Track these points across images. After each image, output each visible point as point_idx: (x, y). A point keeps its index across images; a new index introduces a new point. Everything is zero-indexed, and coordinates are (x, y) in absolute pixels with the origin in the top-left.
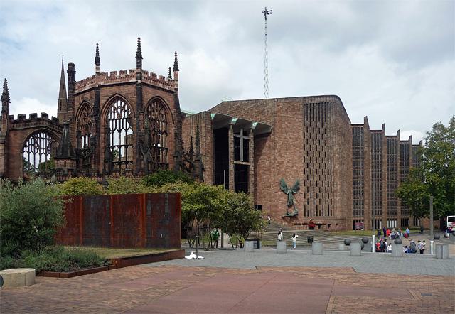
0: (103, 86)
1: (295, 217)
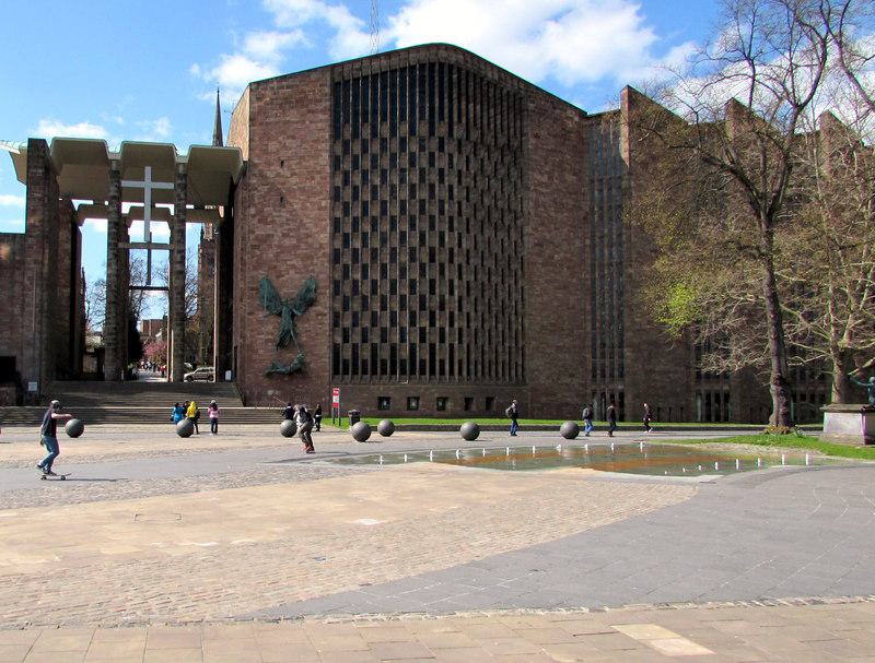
1: (299, 372)
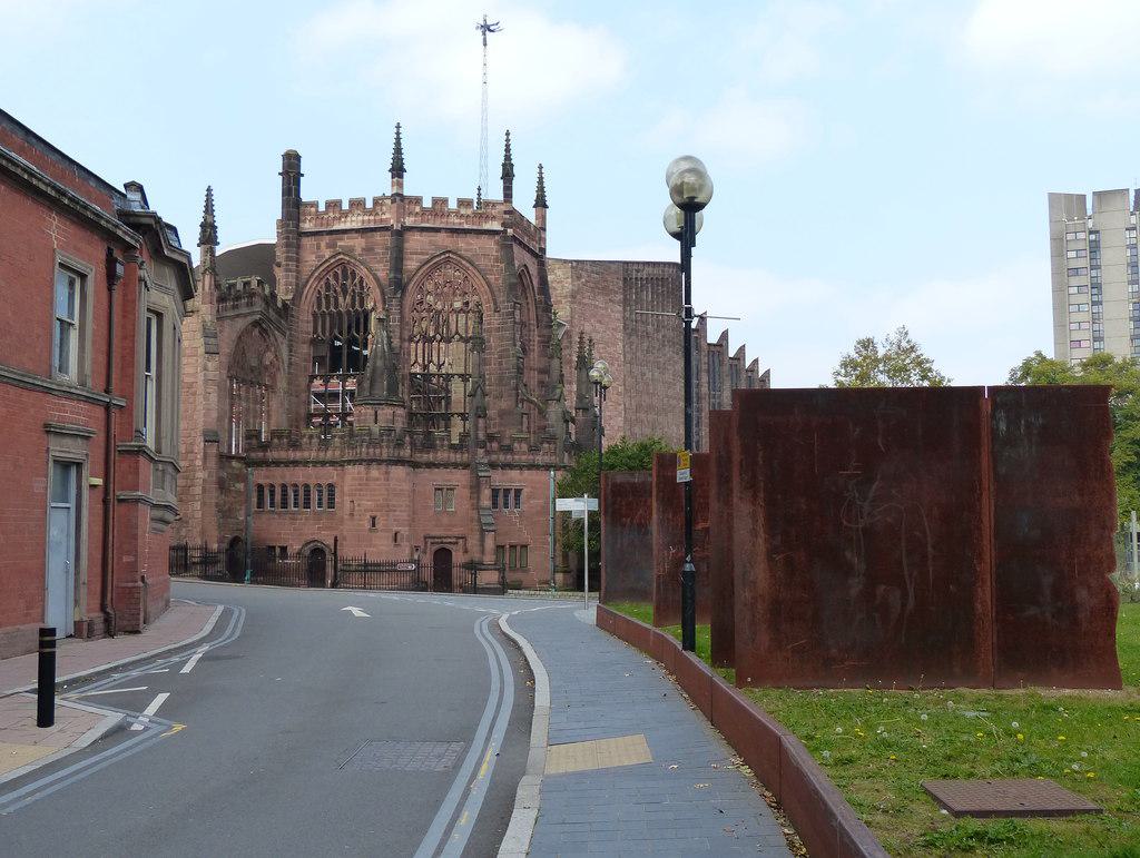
0: (411, 229)
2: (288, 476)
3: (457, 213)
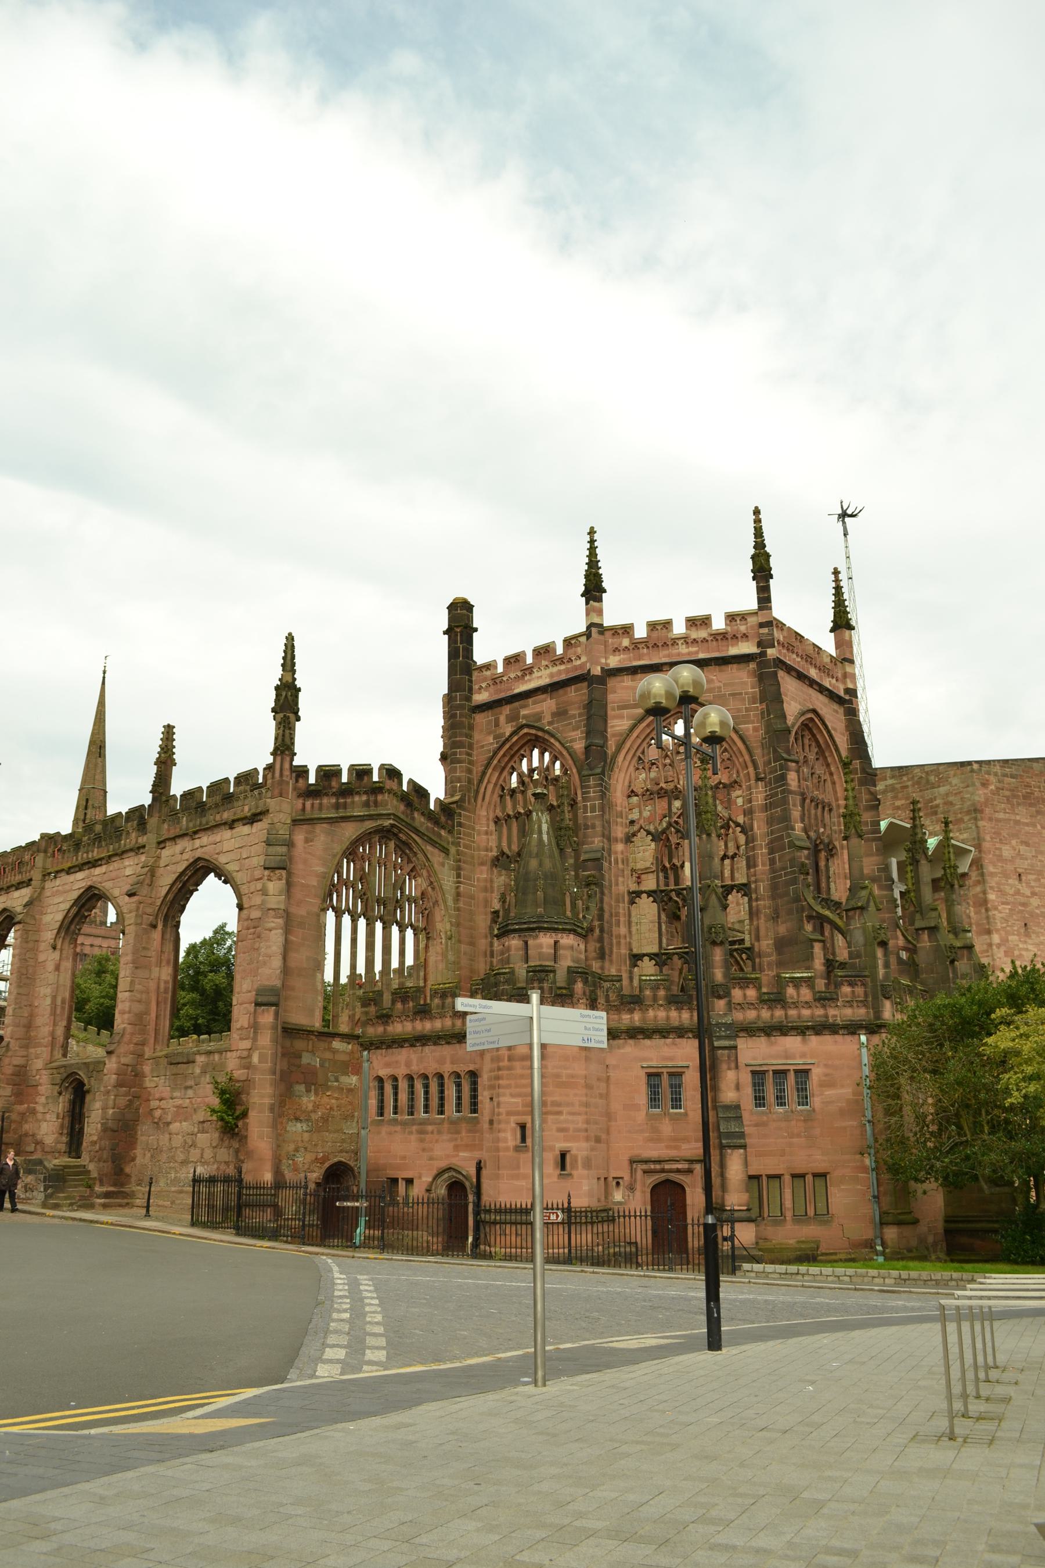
2: (415, 1062)
3: (685, 639)
